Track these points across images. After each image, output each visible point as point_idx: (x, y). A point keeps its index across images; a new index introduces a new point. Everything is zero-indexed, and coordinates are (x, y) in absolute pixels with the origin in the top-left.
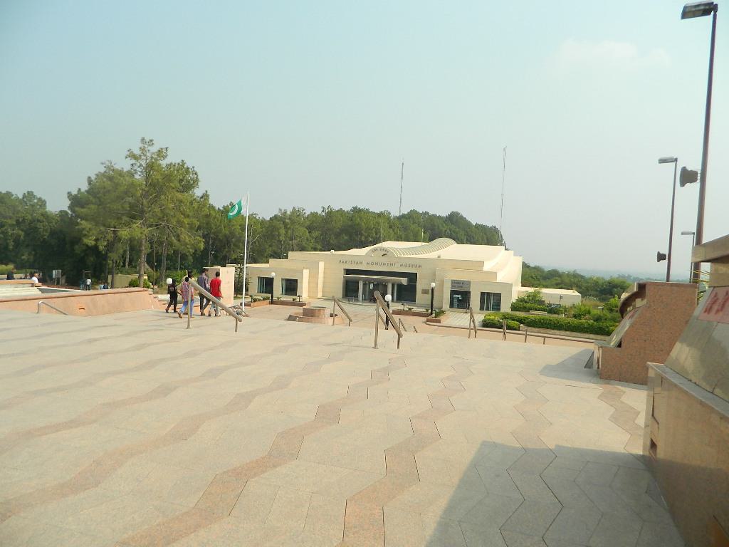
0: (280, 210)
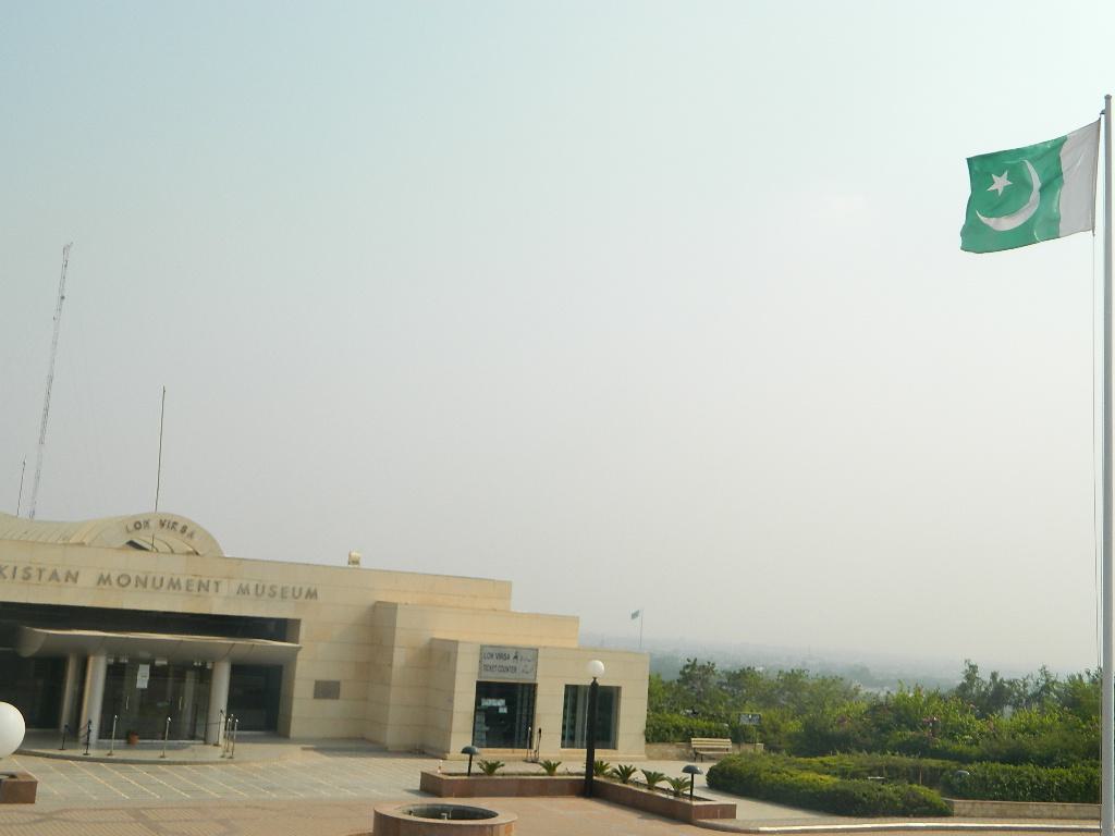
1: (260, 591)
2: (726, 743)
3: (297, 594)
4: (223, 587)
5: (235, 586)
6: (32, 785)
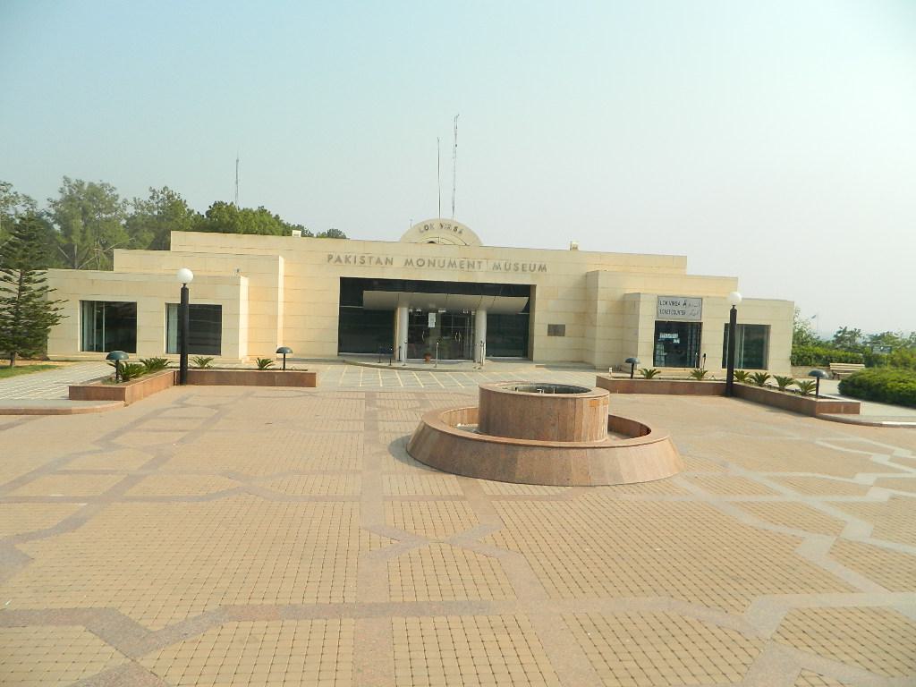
0: (67, 180)
2: (860, 367)
3: (532, 268)
4: (484, 266)
5: (491, 264)
6: (313, 375)
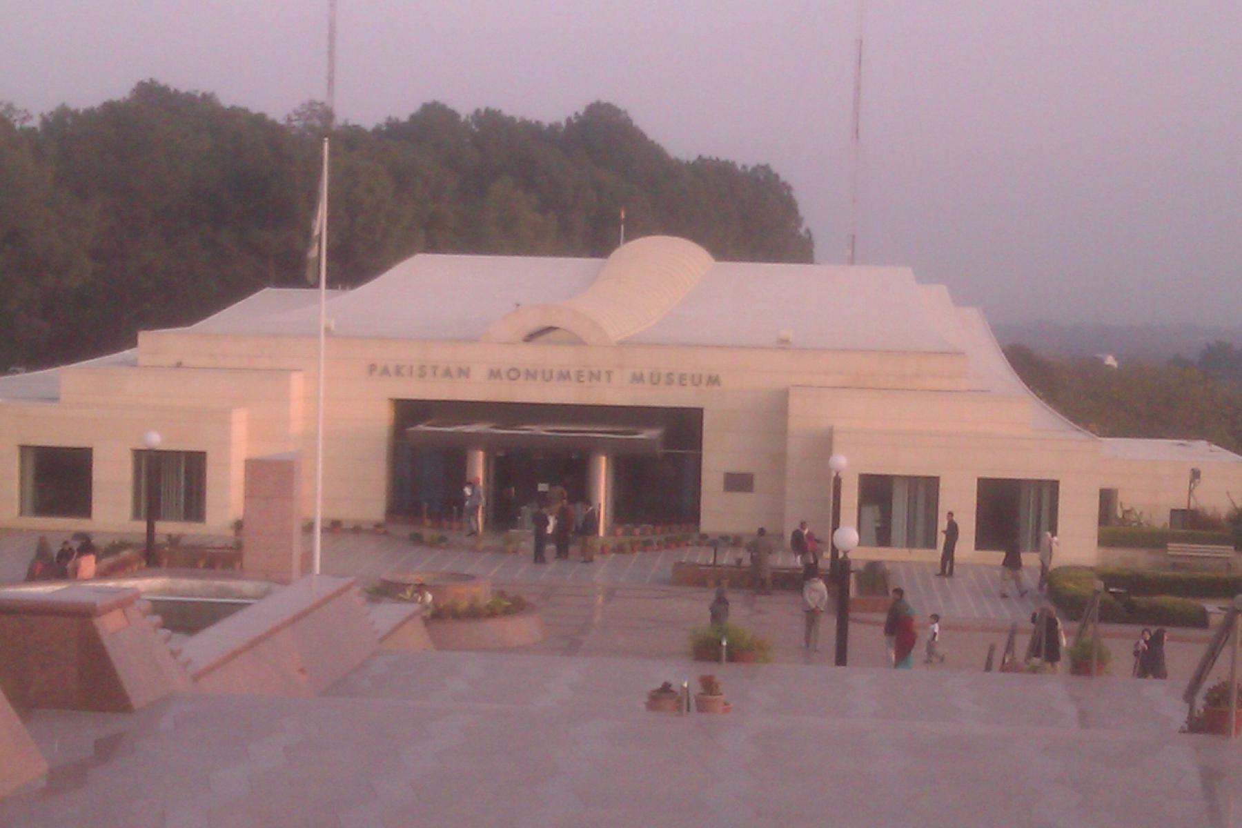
1: (655, 379)
